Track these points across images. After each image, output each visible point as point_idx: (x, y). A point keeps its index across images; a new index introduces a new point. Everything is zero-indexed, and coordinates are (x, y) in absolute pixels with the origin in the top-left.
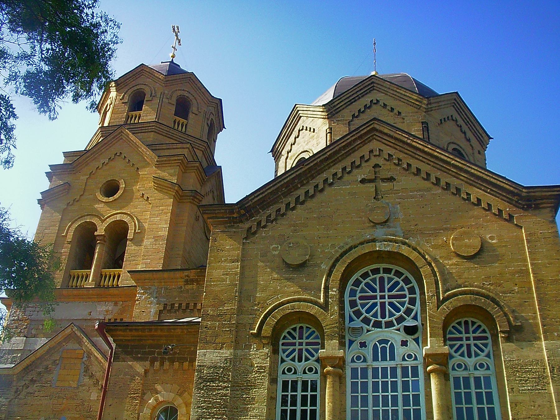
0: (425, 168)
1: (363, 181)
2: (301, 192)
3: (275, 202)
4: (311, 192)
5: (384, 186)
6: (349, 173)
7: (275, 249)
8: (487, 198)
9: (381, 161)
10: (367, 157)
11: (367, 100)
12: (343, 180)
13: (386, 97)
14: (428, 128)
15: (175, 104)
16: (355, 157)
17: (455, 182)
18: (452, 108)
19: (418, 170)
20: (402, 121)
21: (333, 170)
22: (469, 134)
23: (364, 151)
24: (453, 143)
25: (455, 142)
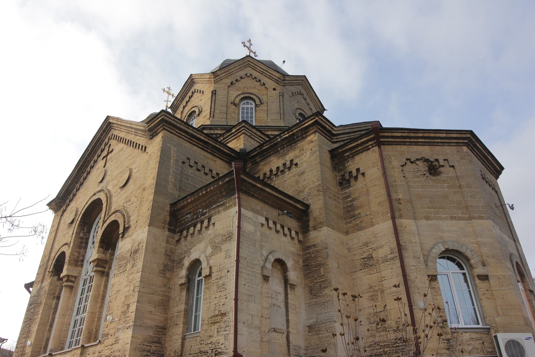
11: (190, 94)
24: (243, 94)
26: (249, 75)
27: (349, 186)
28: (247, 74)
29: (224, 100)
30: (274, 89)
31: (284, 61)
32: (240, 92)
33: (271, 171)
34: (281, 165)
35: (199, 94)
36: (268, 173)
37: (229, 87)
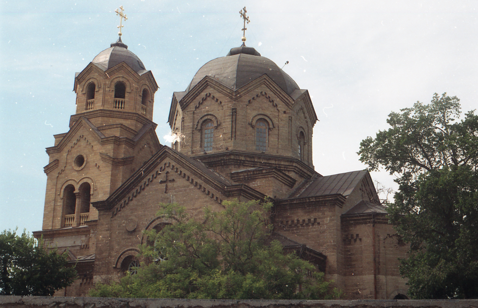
0: (188, 173)
1: (162, 182)
2: (134, 191)
3: (124, 197)
4: (139, 190)
5: (170, 184)
6: (156, 178)
7: (124, 223)
8: (213, 191)
9: (169, 170)
10: (163, 168)
11: (203, 94)
12: (153, 182)
13: (215, 91)
14: (236, 112)
15: (114, 89)
16: (158, 169)
17: (199, 181)
18: (263, 86)
19: (185, 174)
20: (221, 108)
21: (148, 177)
22: (277, 101)
23: (162, 165)
24: (259, 115)
25: (262, 113)
26: (264, 93)
27: (350, 244)
28: (262, 92)
29: (243, 120)
30: (285, 112)
31: (288, 62)
32: (255, 113)
33: (298, 221)
34: (306, 220)
35: (214, 102)
36: (296, 221)
37: (247, 105)
